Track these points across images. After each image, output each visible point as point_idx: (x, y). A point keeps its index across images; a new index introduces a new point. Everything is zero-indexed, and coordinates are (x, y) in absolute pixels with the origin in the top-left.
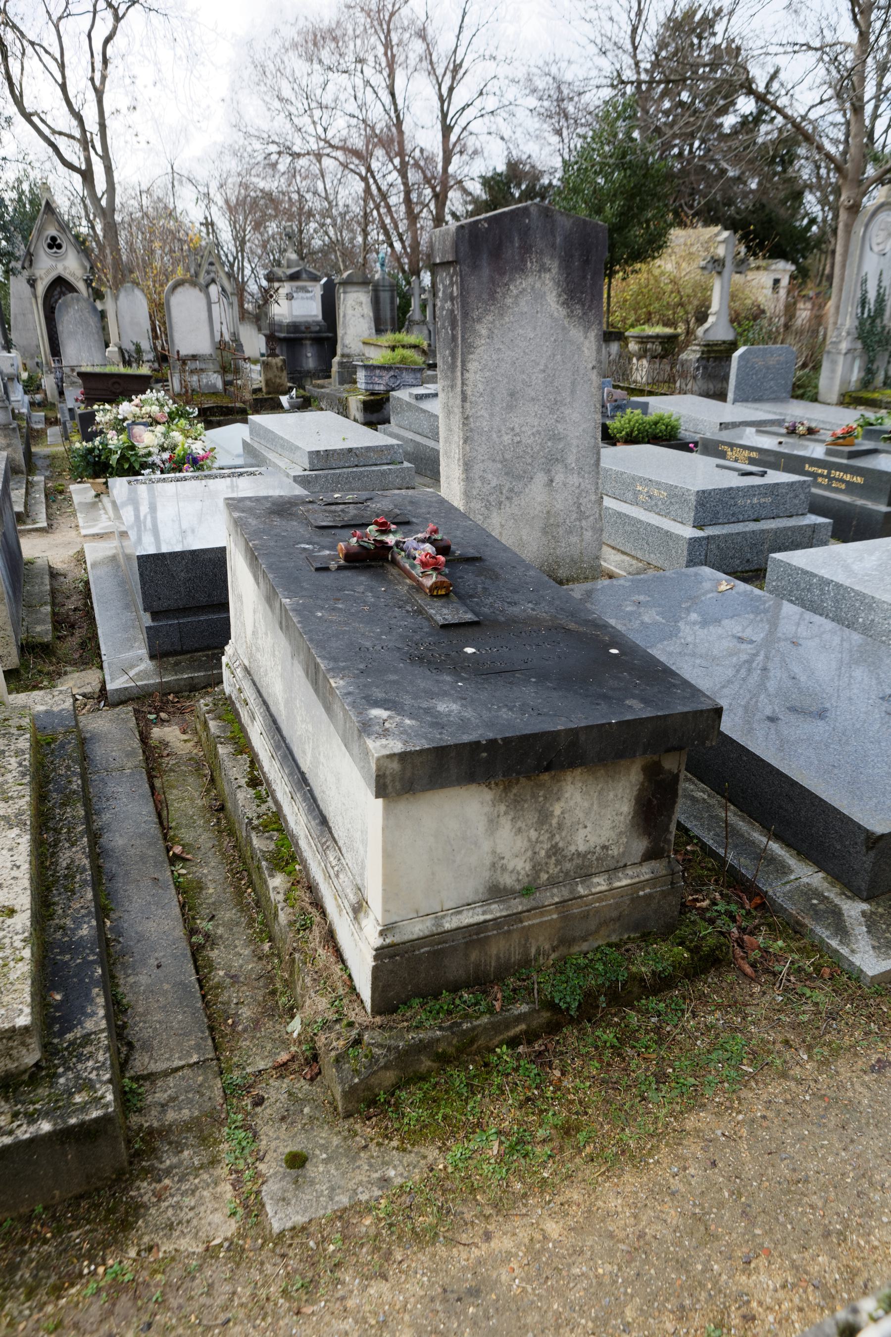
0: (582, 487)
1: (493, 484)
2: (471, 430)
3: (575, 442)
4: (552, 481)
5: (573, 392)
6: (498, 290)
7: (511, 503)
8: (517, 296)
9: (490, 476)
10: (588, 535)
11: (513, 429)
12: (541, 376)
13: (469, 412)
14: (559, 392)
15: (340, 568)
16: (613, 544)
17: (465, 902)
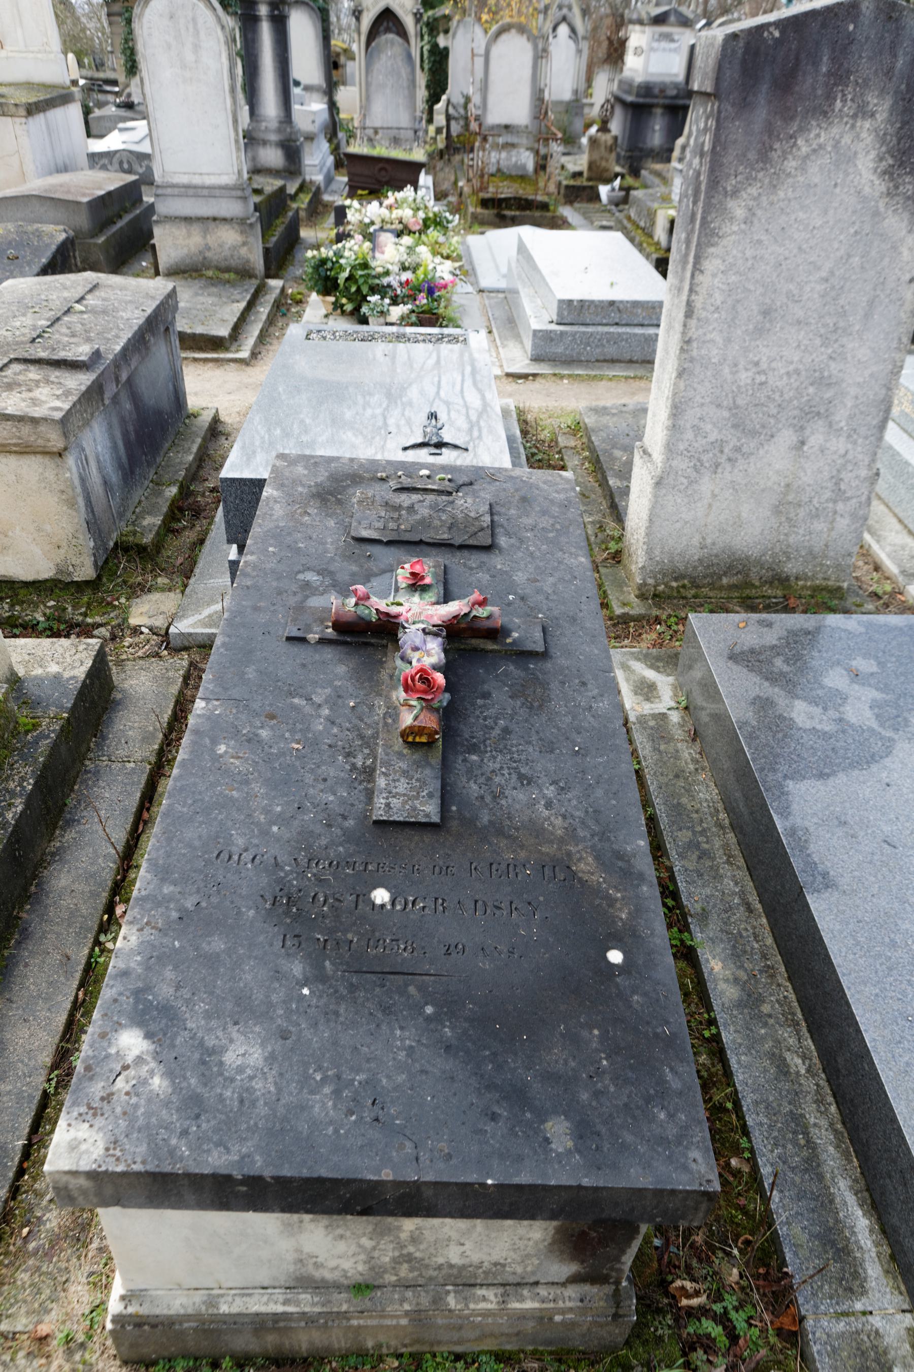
0: (850, 456)
1: (712, 437)
2: (692, 360)
3: (853, 391)
4: (803, 443)
5: (867, 316)
6: (777, 146)
7: (733, 467)
8: (807, 157)
9: (708, 427)
10: (843, 523)
11: (757, 364)
12: (820, 288)
13: (693, 333)
14: (844, 314)
15: (323, 641)
16: (901, 515)
17: (258, 1284)
